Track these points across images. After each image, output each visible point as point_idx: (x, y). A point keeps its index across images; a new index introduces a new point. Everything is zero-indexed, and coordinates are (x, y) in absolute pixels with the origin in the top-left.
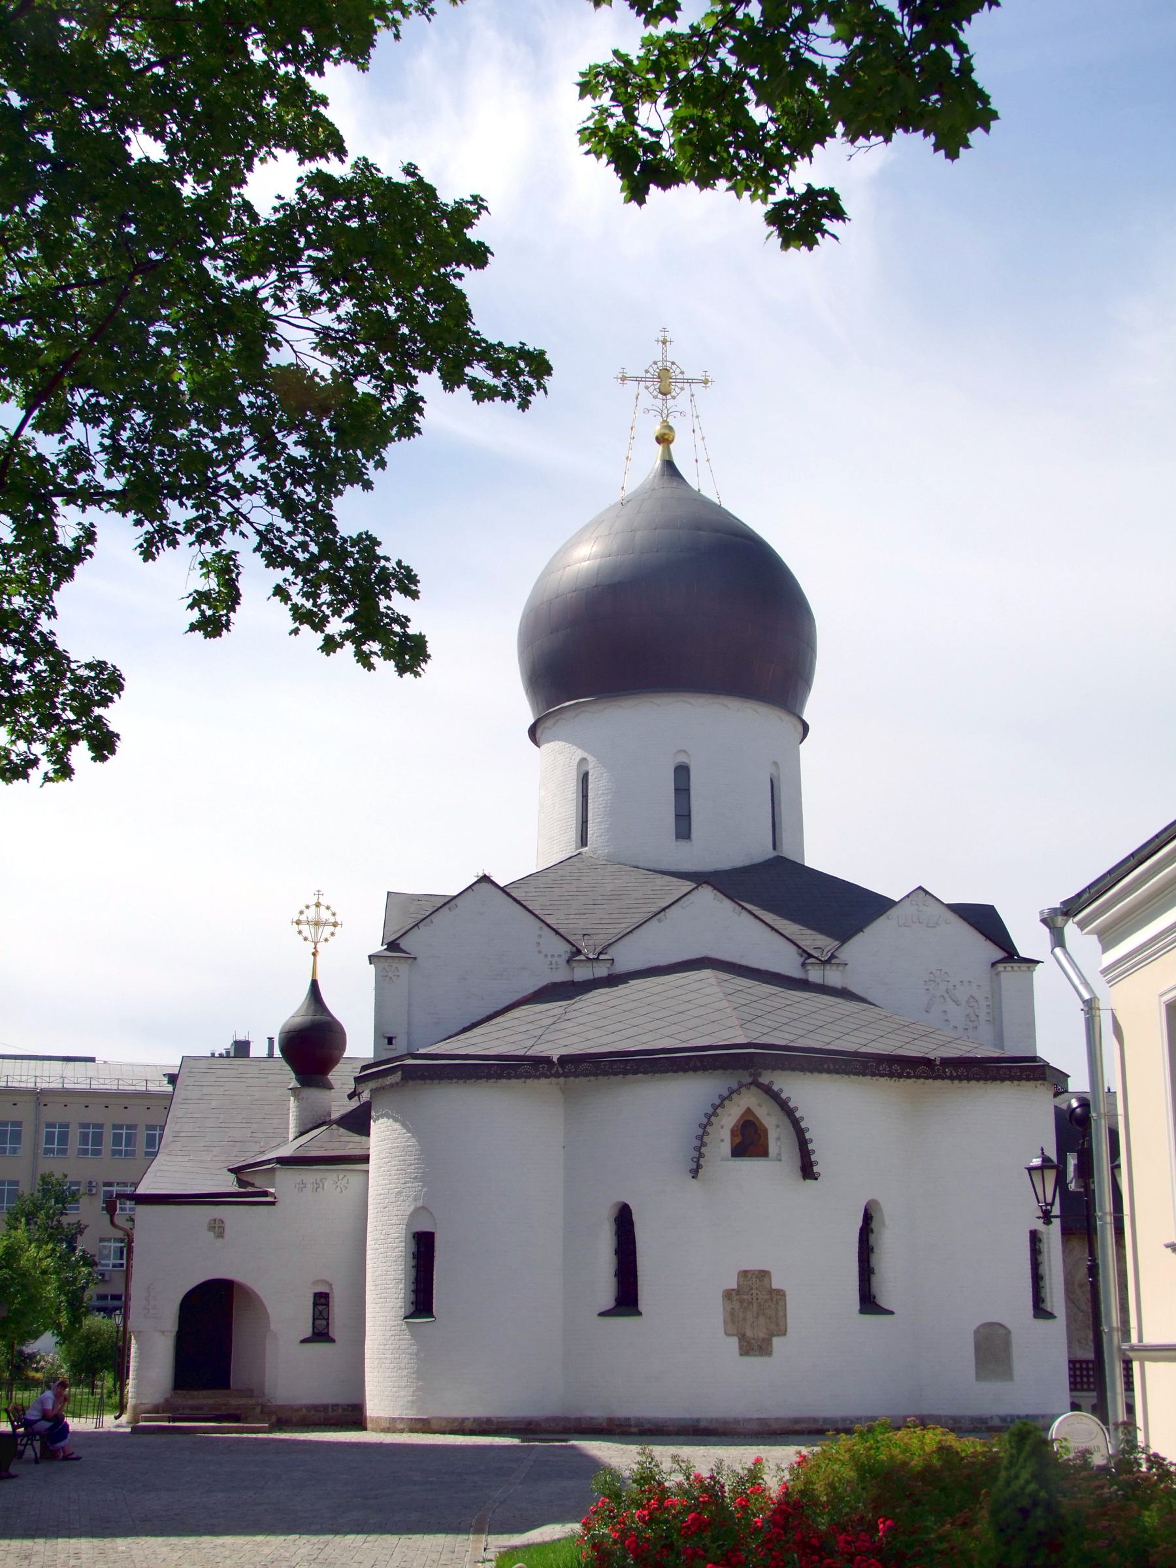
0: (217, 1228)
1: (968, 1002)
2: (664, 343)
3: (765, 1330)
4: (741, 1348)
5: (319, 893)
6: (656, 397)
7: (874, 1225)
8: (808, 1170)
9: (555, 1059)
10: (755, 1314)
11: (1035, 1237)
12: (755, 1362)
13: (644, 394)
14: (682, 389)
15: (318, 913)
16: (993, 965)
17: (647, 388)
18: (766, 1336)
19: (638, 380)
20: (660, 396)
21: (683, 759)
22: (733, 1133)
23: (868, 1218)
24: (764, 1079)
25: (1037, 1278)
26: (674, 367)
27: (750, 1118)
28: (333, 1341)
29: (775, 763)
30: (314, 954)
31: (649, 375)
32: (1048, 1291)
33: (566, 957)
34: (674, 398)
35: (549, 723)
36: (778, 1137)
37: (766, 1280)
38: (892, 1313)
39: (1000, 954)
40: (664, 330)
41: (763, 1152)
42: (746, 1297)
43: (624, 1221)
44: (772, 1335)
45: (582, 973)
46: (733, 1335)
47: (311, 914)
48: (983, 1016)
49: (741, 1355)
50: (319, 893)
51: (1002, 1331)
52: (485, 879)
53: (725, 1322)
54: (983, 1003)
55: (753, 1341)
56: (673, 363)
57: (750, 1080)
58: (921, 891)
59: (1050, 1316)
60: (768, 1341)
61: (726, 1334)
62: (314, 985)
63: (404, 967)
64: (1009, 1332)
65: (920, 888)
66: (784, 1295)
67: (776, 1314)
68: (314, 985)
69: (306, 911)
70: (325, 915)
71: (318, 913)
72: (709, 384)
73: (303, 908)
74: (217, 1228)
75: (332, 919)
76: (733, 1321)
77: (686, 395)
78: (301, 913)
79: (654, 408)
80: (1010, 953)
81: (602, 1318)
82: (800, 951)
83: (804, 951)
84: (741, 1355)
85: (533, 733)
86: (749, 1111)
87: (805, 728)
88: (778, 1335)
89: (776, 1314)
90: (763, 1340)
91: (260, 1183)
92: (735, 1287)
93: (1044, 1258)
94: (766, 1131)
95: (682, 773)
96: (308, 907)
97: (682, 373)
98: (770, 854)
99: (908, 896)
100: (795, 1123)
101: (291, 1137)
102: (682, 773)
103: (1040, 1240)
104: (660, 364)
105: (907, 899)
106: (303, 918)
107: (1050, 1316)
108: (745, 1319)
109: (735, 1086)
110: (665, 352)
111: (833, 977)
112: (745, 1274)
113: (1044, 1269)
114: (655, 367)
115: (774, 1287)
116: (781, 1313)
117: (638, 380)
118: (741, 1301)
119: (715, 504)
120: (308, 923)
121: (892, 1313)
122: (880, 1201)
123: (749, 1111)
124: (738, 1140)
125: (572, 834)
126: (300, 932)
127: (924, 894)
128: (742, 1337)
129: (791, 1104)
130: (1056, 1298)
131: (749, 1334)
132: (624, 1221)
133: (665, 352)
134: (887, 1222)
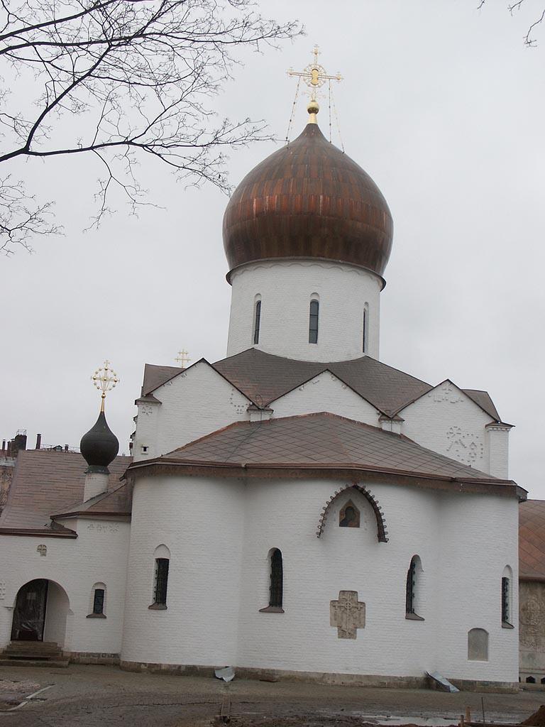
0: (42, 550)
1: (470, 446)
2: (316, 54)
5: (107, 362)
6: (309, 86)
7: (415, 570)
8: (382, 536)
9: (243, 466)
11: (505, 581)
12: (348, 642)
13: (302, 81)
14: (324, 82)
15: (106, 374)
16: (486, 426)
17: (304, 80)
19: (300, 75)
21: (315, 298)
22: (341, 514)
23: (413, 565)
24: (361, 486)
25: (505, 605)
26: (321, 69)
28: (105, 617)
29: (366, 303)
30: (103, 397)
31: (306, 73)
32: (510, 612)
33: (246, 407)
34: (319, 87)
35: (238, 273)
36: (365, 517)
38: (423, 620)
39: (490, 421)
40: (316, 46)
41: (358, 526)
43: (276, 557)
44: (356, 628)
45: (255, 418)
47: (102, 374)
48: (479, 455)
49: (339, 638)
50: (107, 362)
51: (483, 633)
52: (203, 360)
53: (331, 619)
54: (479, 448)
57: (350, 485)
58: (448, 383)
59: (511, 627)
60: (355, 632)
62: (102, 416)
63: (155, 409)
64: (488, 634)
65: (448, 380)
68: (102, 416)
69: (99, 372)
70: (110, 375)
71: (106, 374)
73: (97, 370)
74: (42, 550)
75: (114, 378)
76: (335, 619)
77: (325, 87)
78: (97, 373)
80: (497, 421)
81: (262, 614)
82: (378, 412)
83: (380, 412)
85: (229, 278)
86: (350, 502)
87: (384, 283)
91: (68, 525)
93: (509, 594)
94: (359, 513)
95: (315, 305)
96: (100, 370)
97: (325, 73)
98: (361, 355)
100: (376, 510)
101: (86, 498)
102: (315, 305)
103: (507, 584)
104: (313, 66)
106: (97, 376)
107: (511, 627)
108: (342, 618)
109: (344, 488)
111: (396, 428)
113: (509, 601)
117: (300, 75)
118: (340, 607)
119: (340, 152)
120: (100, 379)
123: (350, 502)
124: (344, 517)
125: (250, 336)
126: (95, 384)
128: (340, 627)
129: (375, 500)
130: (514, 617)
131: (344, 627)
132: (276, 557)
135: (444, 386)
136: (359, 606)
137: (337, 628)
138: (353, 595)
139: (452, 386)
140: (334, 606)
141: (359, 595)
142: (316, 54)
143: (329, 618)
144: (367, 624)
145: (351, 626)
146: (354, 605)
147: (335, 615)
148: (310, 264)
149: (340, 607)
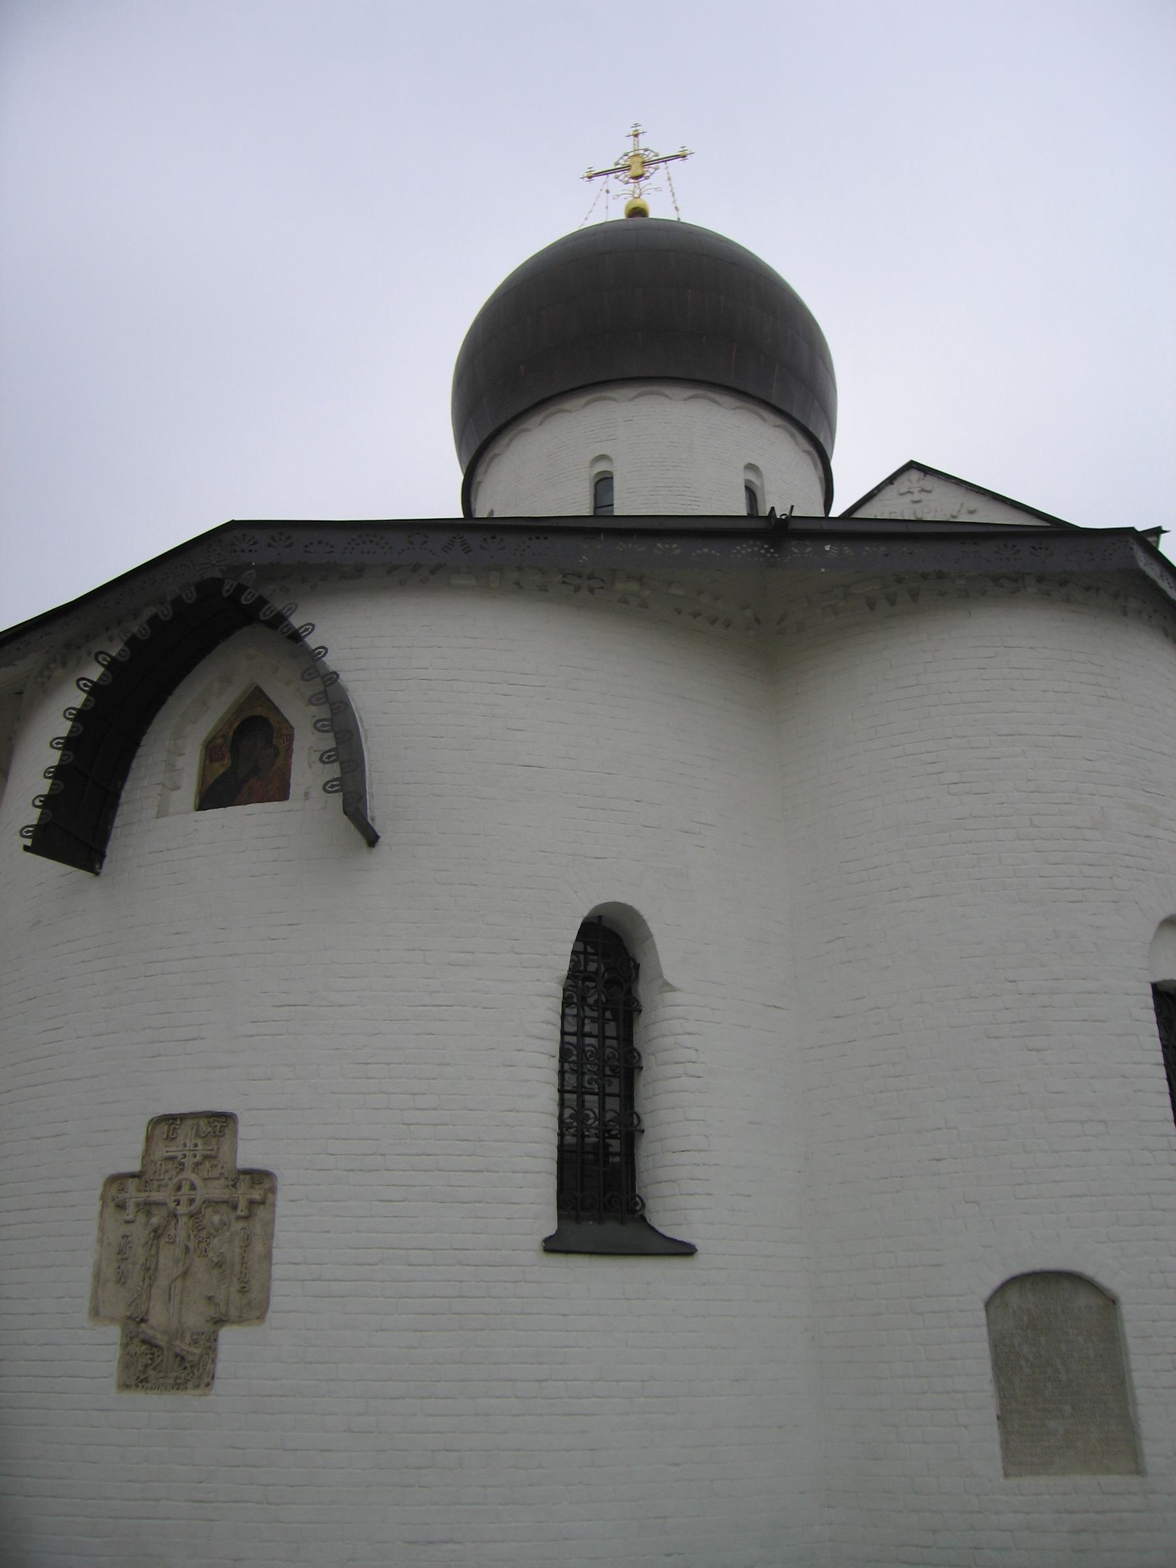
4: (127, 1364)
19: (606, 173)
20: (632, 181)
21: (602, 467)
22: (211, 751)
27: (259, 711)
29: (751, 467)
34: (647, 178)
38: (685, 1250)
46: (112, 1320)
49: (125, 1386)
51: (1084, 1300)
53: (97, 1276)
55: (162, 1340)
56: (646, 150)
58: (914, 475)
64: (1110, 1302)
66: (273, 1190)
72: (688, 157)
76: (121, 1279)
79: (624, 192)
84: (125, 1386)
86: (257, 695)
88: (241, 1320)
92: (136, 1167)
99: (891, 480)
105: (891, 487)
110: (636, 144)
112: (170, 1122)
114: (626, 158)
116: (258, 1247)
118: (147, 1207)
121: (685, 1250)
122: (646, 910)
124: (219, 769)
127: (921, 475)
133: (636, 144)
134: (668, 974)
135: (902, 484)
136: (245, 1192)
137: (114, 1333)
138: (219, 1135)
139: (929, 482)
140: (121, 1206)
141: (242, 1130)
142: (636, 136)
143: (88, 1272)
144: (281, 1294)
145: (195, 1318)
146: (217, 1190)
147: (122, 1252)
148: (583, 400)
149: (147, 1207)
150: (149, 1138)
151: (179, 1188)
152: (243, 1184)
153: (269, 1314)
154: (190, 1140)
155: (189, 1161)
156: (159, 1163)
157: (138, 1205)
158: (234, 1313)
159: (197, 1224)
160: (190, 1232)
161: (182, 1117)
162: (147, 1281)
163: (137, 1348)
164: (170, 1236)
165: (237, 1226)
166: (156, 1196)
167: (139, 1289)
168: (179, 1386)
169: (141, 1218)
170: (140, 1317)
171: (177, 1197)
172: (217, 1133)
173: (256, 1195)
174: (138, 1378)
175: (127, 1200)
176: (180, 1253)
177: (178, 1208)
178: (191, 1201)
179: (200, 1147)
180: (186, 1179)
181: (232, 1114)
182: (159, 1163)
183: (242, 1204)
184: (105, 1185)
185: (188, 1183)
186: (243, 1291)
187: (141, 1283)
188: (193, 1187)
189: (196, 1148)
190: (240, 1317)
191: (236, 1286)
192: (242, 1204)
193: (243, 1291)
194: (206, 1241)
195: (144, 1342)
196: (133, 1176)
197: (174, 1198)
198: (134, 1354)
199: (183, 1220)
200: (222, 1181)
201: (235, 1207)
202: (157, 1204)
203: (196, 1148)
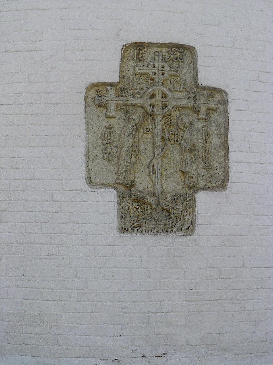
3: (178, 176)
4: (123, 213)
10: (157, 140)
18: (184, 191)
37: (186, 69)
42: (138, 101)
44: (194, 188)
49: (123, 230)
55: (152, 201)
61: (90, 181)
66: (225, 102)
67: (205, 143)
76: (108, 156)
84: (123, 230)
88: (207, 188)
89: (205, 143)
90: (175, 198)
92: (115, 78)
115: (202, 82)
116: (215, 141)
143: (82, 151)
147: (106, 139)
150: (122, 58)
151: (153, 96)
152: (202, 97)
153: (229, 184)
154: (158, 63)
155: (159, 78)
156: (131, 77)
157: (117, 106)
158: (202, 183)
159: (169, 122)
160: (164, 127)
161: (150, 45)
162: (133, 159)
163: (127, 203)
164: (148, 130)
165: (200, 125)
166: (132, 101)
167: (127, 164)
168: (167, 230)
169: (121, 115)
170: (131, 184)
171: (152, 102)
172: (178, 59)
173: (213, 106)
174: (133, 224)
175: (109, 102)
176: (159, 141)
177: (154, 110)
178: (164, 107)
179: (167, 68)
180: (158, 90)
181: (192, 47)
182: (131, 77)
183: (203, 110)
184: (86, 90)
185: (160, 93)
186: (208, 167)
187: (129, 161)
188: (164, 96)
189: (163, 69)
190: (206, 185)
191: (202, 165)
192: (203, 110)
193: (208, 167)
194: (177, 134)
195: (135, 201)
196: (111, 84)
197: (149, 103)
198: (127, 209)
199: (158, 119)
200: (185, 93)
201: (197, 112)
202: (133, 106)
203: (163, 69)
